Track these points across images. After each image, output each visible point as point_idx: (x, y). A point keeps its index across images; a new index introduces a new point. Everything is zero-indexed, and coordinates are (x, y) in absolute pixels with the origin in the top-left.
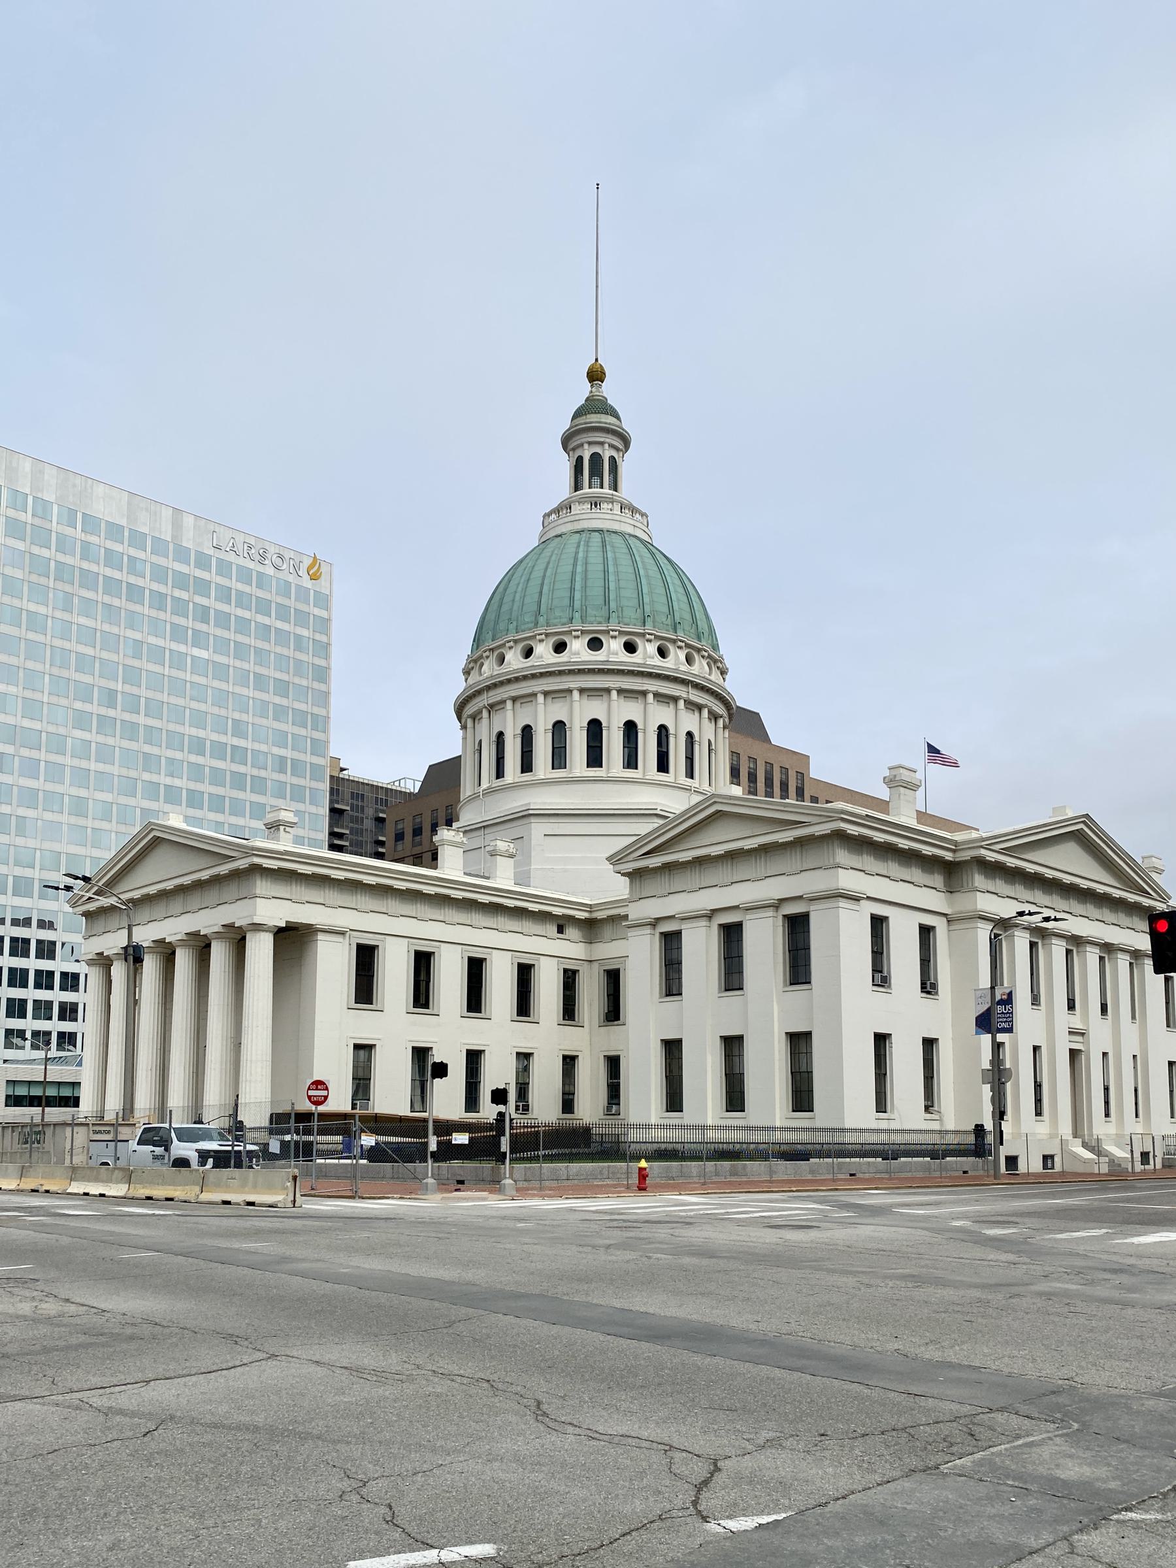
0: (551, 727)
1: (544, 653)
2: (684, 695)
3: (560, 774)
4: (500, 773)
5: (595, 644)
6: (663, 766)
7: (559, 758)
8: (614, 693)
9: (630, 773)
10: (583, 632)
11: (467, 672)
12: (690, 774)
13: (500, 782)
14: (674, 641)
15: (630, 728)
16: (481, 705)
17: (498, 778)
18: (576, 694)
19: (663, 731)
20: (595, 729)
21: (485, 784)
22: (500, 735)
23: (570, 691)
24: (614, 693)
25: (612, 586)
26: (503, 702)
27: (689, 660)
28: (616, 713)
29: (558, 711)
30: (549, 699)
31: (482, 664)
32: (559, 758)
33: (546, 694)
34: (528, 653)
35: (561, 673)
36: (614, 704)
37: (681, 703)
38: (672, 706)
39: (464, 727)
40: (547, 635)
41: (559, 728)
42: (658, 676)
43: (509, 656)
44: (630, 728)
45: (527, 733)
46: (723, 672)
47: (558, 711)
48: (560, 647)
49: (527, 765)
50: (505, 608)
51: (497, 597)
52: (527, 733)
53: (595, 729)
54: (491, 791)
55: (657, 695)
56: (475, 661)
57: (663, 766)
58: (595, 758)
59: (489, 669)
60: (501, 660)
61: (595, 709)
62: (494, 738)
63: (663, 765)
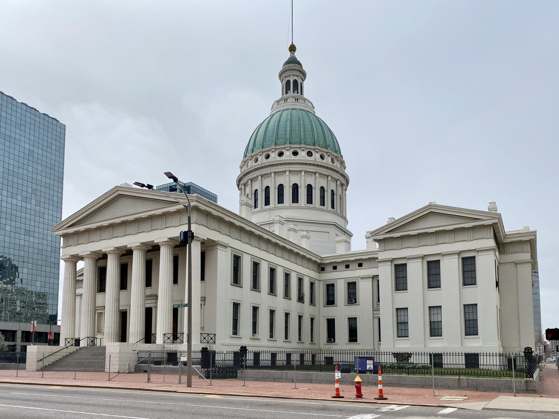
0: (277, 186)
1: (274, 156)
2: (331, 174)
3: (281, 205)
5: (295, 153)
6: (323, 203)
7: (281, 200)
8: (303, 173)
10: (290, 148)
14: (327, 153)
15: (310, 188)
16: (248, 179)
17: (255, 208)
18: (287, 173)
19: (322, 188)
20: (295, 188)
22: (256, 190)
24: (303, 173)
26: (257, 177)
27: (333, 161)
28: (303, 182)
29: (280, 180)
30: (276, 176)
32: (281, 200)
34: (268, 157)
35: (281, 164)
36: (303, 177)
37: (329, 178)
38: (326, 179)
40: (276, 149)
42: (321, 166)
43: (260, 158)
44: (310, 188)
45: (267, 188)
47: (280, 180)
48: (281, 154)
49: (267, 202)
53: (295, 188)
55: (320, 174)
56: (245, 162)
57: (323, 203)
58: (295, 199)
59: (252, 164)
60: (257, 160)
61: (295, 179)
62: (253, 192)
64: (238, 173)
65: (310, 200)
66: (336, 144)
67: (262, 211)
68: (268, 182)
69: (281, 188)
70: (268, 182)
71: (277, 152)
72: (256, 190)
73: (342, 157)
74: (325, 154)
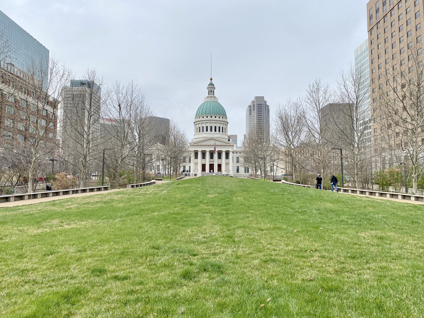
5: (211, 117)
7: (207, 130)
15: (215, 127)
19: (219, 127)
20: (211, 127)
27: (223, 118)
32: (207, 130)
34: (203, 117)
41: (207, 127)
44: (215, 127)
47: (207, 125)
48: (207, 117)
53: (211, 127)
58: (211, 130)
61: (211, 125)
63: (219, 131)
64: (194, 120)
65: (215, 131)
67: (202, 134)
68: (203, 125)
70: (203, 125)
73: (226, 116)
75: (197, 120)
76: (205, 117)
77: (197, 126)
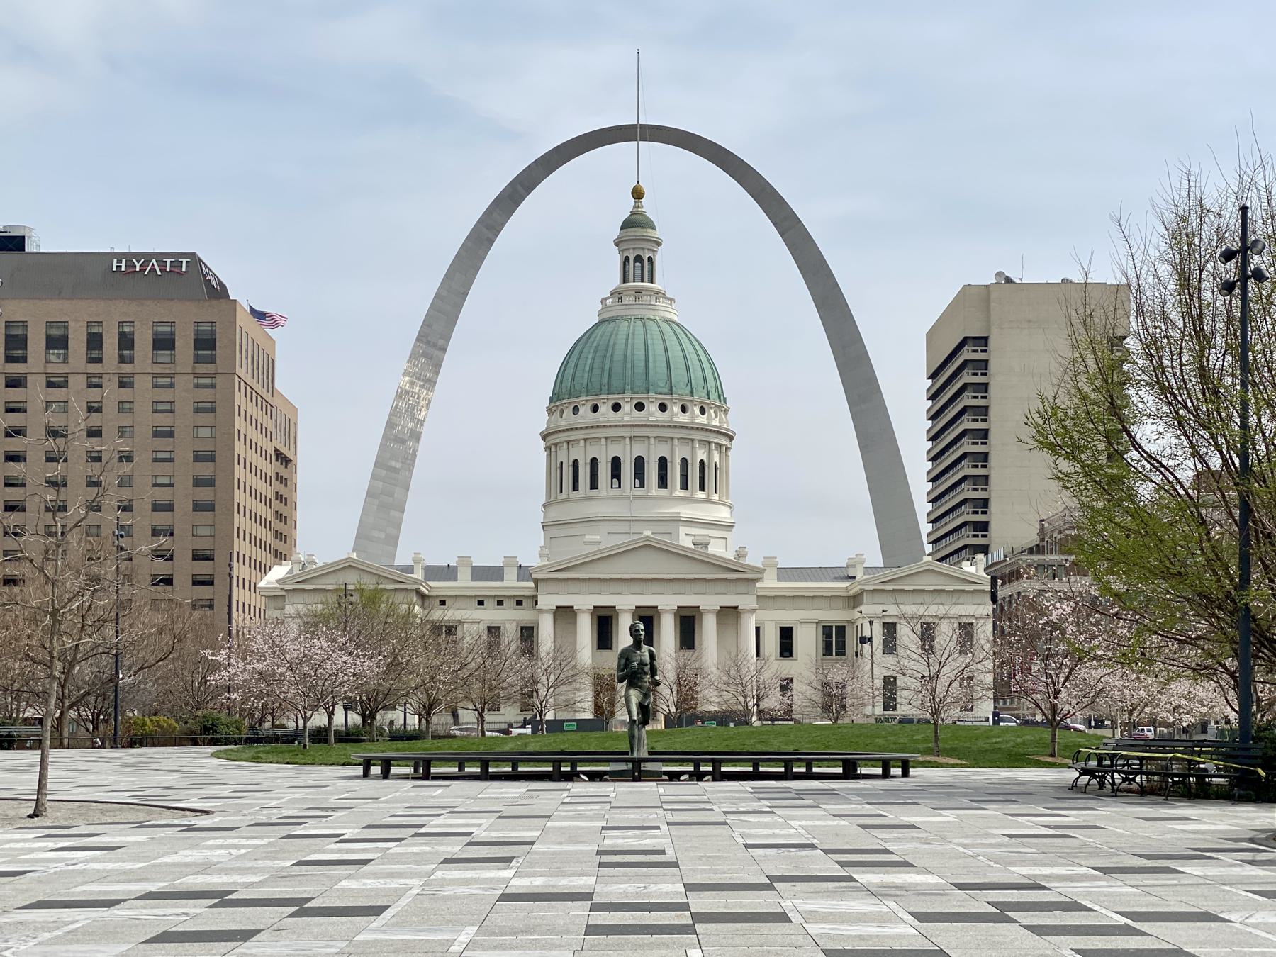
1: (605, 409)
4: (575, 488)
5: (640, 407)
8: (652, 440)
9: (663, 492)
11: (549, 410)
12: (702, 488)
13: (574, 495)
15: (663, 463)
19: (684, 461)
20: (640, 463)
21: (564, 496)
22: (576, 462)
23: (624, 438)
24: (652, 440)
25: (651, 365)
27: (702, 411)
31: (562, 411)
33: (607, 438)
34: (595, 409)
36: (652, 447)
39: (547, 448)
43: (582, 411)
44: (663, 463)
45: (594, 462)
46: (726, 412)
47: (616, 450)
48: (616, 407)
49: (594, 485)
50: (578, 374)
51: (572, 365)
52: (594, 462)
53: (640, 463)
54: (569, 500)
59: (569, 419)
61: (639, 450)
63: (684, 486)
64: (541, 421)
65: (663, 482)
66: (710, 378)
69: (616, 462)
71: (611, 403)
72: (576, 462)
73: (721, 397)
74: (689, 405)
75: (563, 423)
76: (602, 409)
77: (562, 456)
